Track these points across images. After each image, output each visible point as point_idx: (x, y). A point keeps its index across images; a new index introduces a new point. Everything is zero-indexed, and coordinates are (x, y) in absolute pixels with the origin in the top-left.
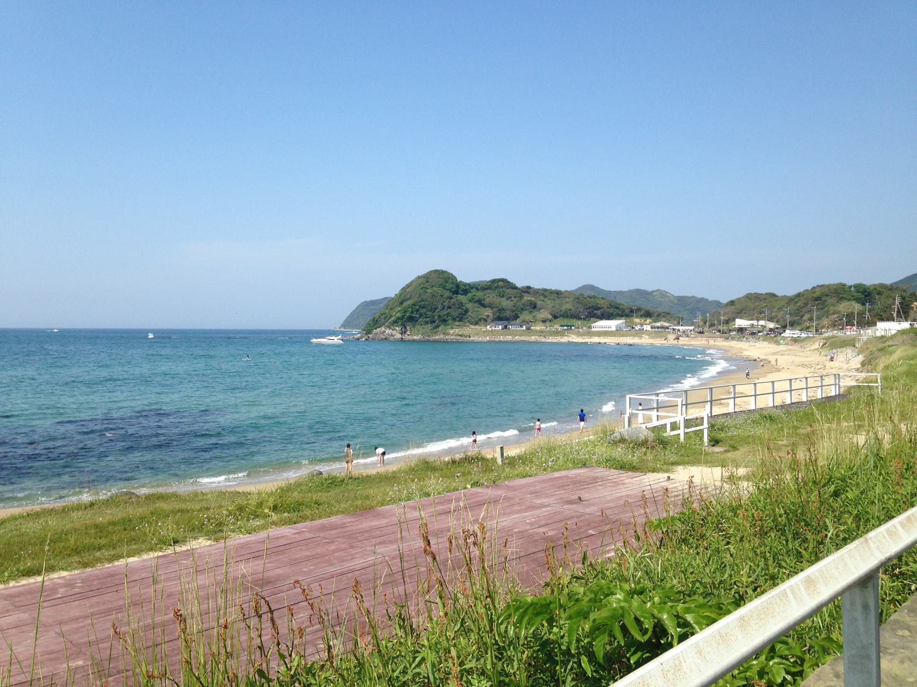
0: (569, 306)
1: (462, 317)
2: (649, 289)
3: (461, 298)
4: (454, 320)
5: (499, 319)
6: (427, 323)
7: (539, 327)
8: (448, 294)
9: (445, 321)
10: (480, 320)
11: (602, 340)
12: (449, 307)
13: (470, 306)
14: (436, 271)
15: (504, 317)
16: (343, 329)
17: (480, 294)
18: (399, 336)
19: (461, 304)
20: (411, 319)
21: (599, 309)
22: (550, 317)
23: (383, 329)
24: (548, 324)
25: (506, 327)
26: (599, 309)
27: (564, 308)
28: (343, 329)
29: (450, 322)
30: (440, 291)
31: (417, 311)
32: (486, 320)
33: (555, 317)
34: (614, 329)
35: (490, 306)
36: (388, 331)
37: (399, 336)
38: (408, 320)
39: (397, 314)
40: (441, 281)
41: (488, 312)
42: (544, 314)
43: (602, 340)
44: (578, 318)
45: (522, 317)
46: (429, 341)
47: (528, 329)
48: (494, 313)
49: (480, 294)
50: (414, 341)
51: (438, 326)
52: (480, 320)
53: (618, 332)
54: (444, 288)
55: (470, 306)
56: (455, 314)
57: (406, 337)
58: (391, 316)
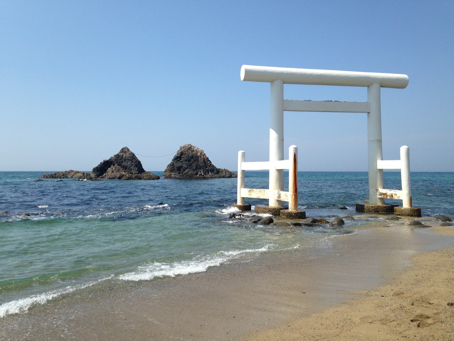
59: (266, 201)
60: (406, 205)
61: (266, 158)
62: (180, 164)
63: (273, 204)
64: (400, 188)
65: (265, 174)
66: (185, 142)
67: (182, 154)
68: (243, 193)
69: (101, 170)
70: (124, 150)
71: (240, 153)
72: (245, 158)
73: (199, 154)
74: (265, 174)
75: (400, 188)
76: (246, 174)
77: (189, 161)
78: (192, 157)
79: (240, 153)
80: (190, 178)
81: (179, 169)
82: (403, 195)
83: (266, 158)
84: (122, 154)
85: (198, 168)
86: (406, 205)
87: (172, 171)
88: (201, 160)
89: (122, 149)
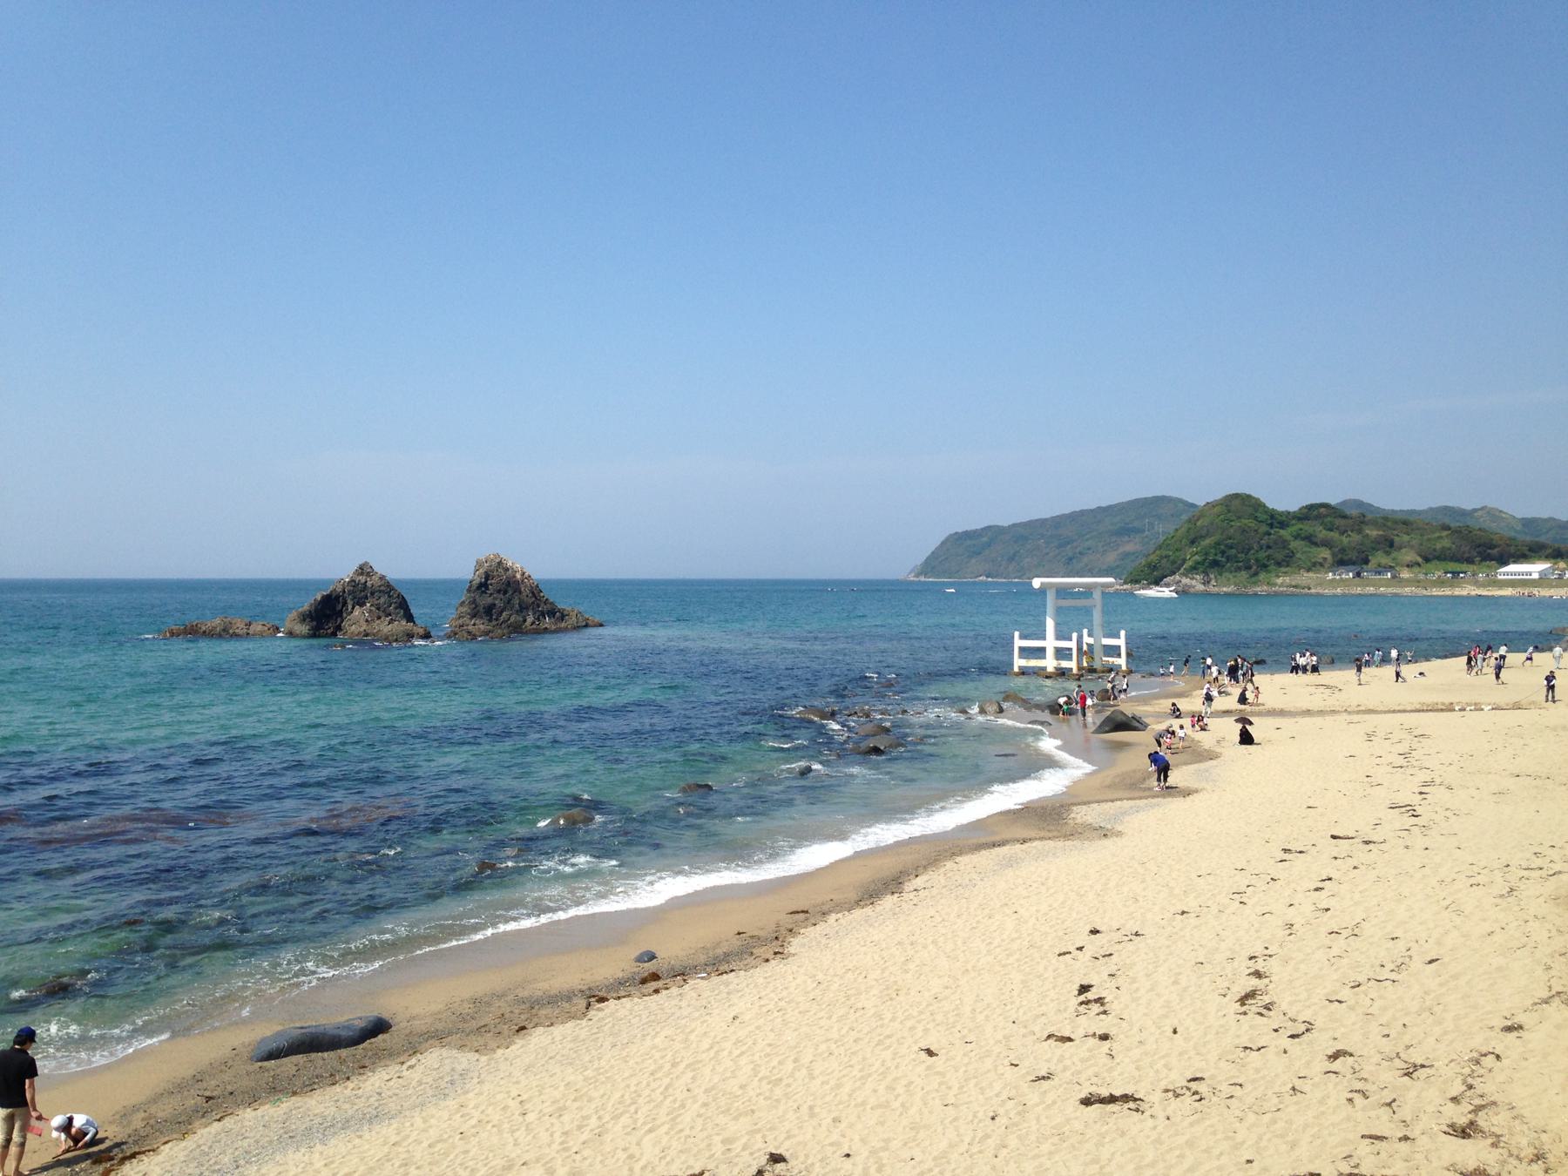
0: (1446, 543)
1: (1287, 561)
2: (1468, 506)
3: (1282, 532)
4: (1279, 564)
5: (1341, 563)
6: (1239, 569)
7: (1406, 574)
8: (1264, 528)
9: (1265, 566)
10: (1314, 564)
11: (1508, 592)
12: (1269, 547)
13: (1294, 544)
14: (1237, 496)
15: (1353, 560)
16: (922, 579)
17: (1308, 527)
18: (1202, 587)
19: (1284, 544)
20: (1215, 564)
21: (1492, 547)
22: (1420, 560)
23: (1177, 577)
24: (1416, 569)
25: (1358, 575)
26: (1492, 547)
27: (1438, 546)
28: (922, 579)
29: (1272, 567)
30: (1252, 524)
31: (1223, 553)
32: (1322, 565)
33: (1427, 560)
34: (1535, 576)
35: (1326, 544)
36: (1185, 581)
37: (1202, 587)
38: (1211, 565)
39: (1192, 556)
40: (1250, 510)
41: (1325, 553)
42: (1410, 556)
43: (1508, 592)
44: (1470, 561)
45: (1373, 561)
46: (1247, 595)
47: (1394, 577)
48: (1334, 555)
49: (1308, 527)
50: (1227, 595)
51: (1256, 574)
52: (1314, 564)
53: (1543, 581)
54: (1256, 518)
55: (1294, 544)
56: (1279, 556)
57: (1212, 589)
58: (1184, 561)
59: (1044, 669)
60: (1124, 668)
61: (1044, 638)
62: (489, 600)
63: (1050, 669)
64: (1119, 655)
65: (1043, 650)
66: (485, 551)
67: (487, 577)
68: (1019, 663)
69: (327, 614)
70: (364, 570)
71: (1017, 634)
72: (1022, 637)
73: (518, 576)
74: (1043, 650)
75: (1119, 655)
76: (1022, 649)
77: (505, 592)
78: (508, 584)
79: (1017, 634)
80: (517, 630)
81: (489, 610)
82: (1122, 661)
83: (1044, 638)
84: (362, 579)
85: (523, 608)
86: (1124, 668)
87: (474, 616)
88: (525, 591)
89: (361, 568)
